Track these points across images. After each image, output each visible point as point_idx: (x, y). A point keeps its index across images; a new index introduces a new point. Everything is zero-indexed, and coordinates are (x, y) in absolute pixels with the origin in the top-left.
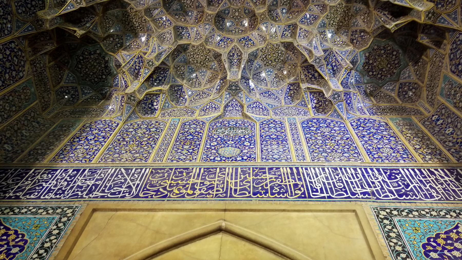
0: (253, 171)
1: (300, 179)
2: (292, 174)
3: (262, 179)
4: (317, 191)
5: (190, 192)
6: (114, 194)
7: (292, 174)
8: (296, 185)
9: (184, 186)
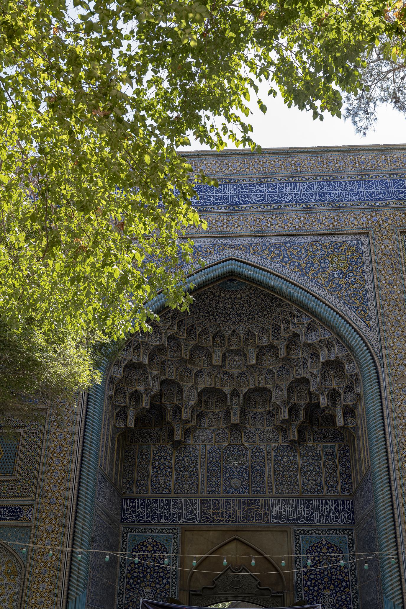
0: (248, 502)
1: (268, 510)
2: (265, 504)
3: (252, 509)
4: (274, 519)
5: (222, 519)
6: (189, 520)
7: (265, 504)
8: (266, 513)
9: (218, 514)
